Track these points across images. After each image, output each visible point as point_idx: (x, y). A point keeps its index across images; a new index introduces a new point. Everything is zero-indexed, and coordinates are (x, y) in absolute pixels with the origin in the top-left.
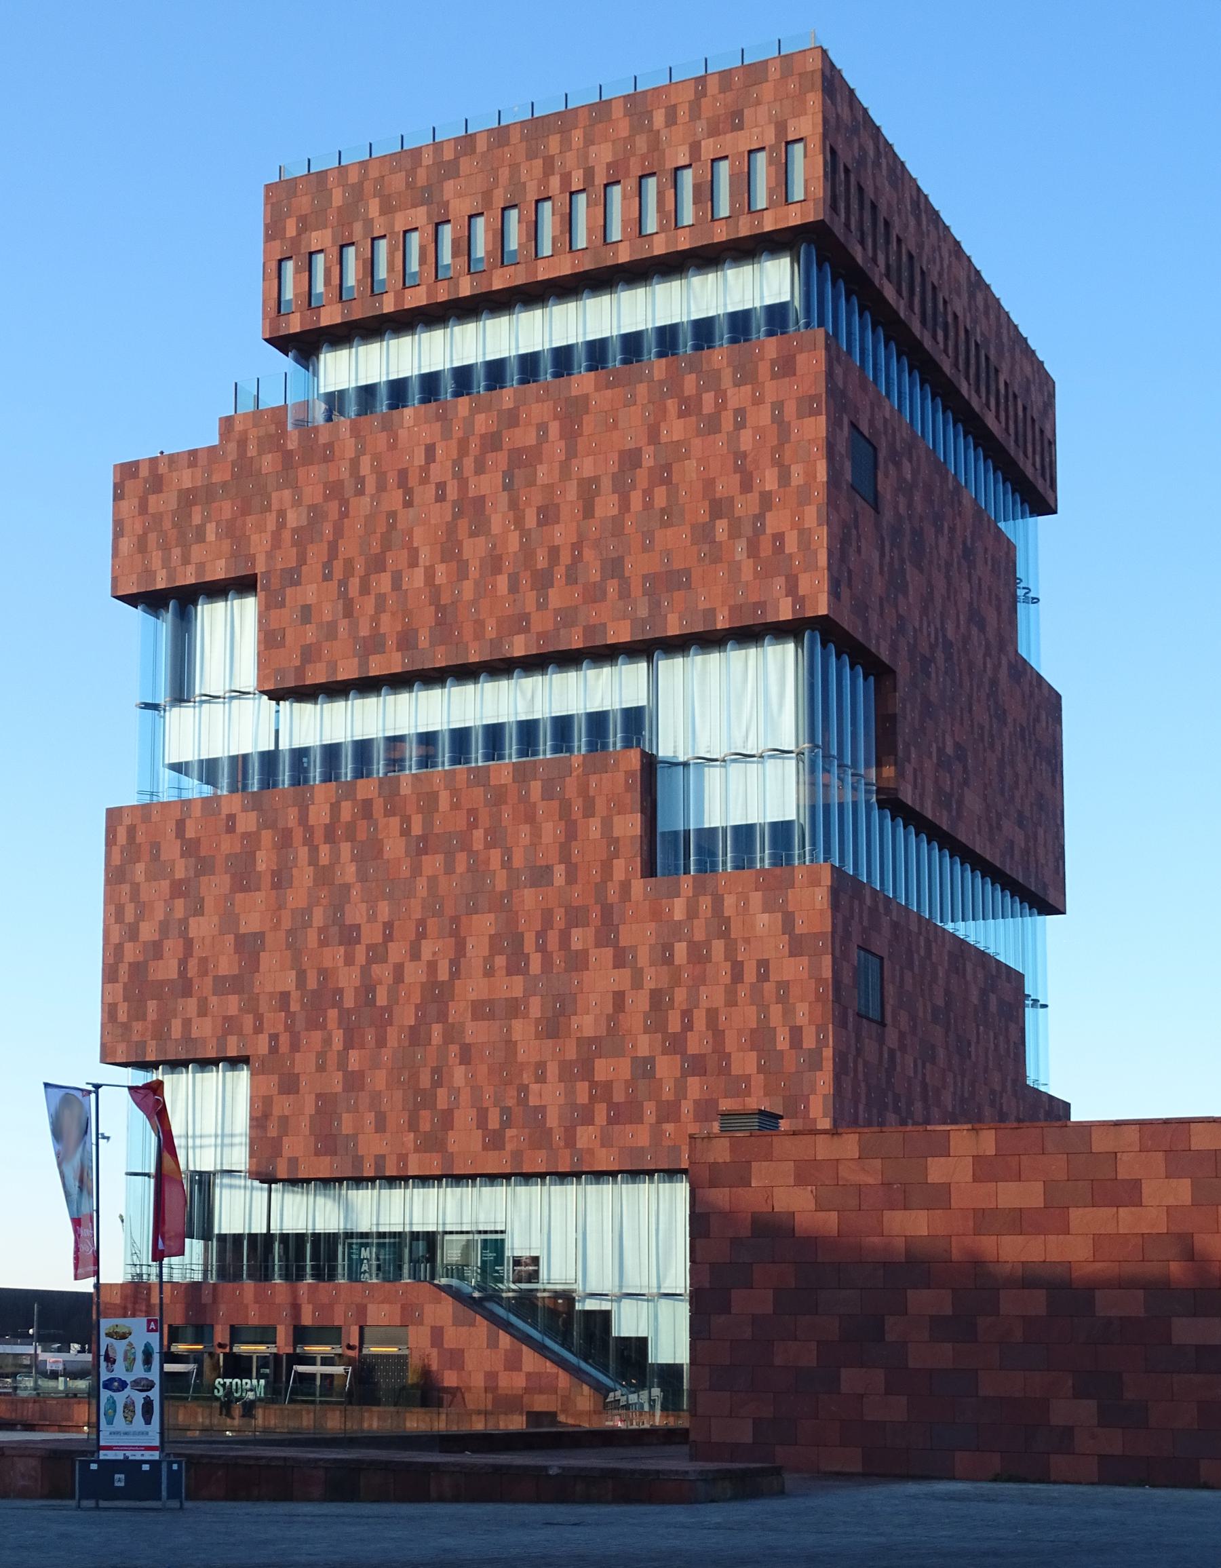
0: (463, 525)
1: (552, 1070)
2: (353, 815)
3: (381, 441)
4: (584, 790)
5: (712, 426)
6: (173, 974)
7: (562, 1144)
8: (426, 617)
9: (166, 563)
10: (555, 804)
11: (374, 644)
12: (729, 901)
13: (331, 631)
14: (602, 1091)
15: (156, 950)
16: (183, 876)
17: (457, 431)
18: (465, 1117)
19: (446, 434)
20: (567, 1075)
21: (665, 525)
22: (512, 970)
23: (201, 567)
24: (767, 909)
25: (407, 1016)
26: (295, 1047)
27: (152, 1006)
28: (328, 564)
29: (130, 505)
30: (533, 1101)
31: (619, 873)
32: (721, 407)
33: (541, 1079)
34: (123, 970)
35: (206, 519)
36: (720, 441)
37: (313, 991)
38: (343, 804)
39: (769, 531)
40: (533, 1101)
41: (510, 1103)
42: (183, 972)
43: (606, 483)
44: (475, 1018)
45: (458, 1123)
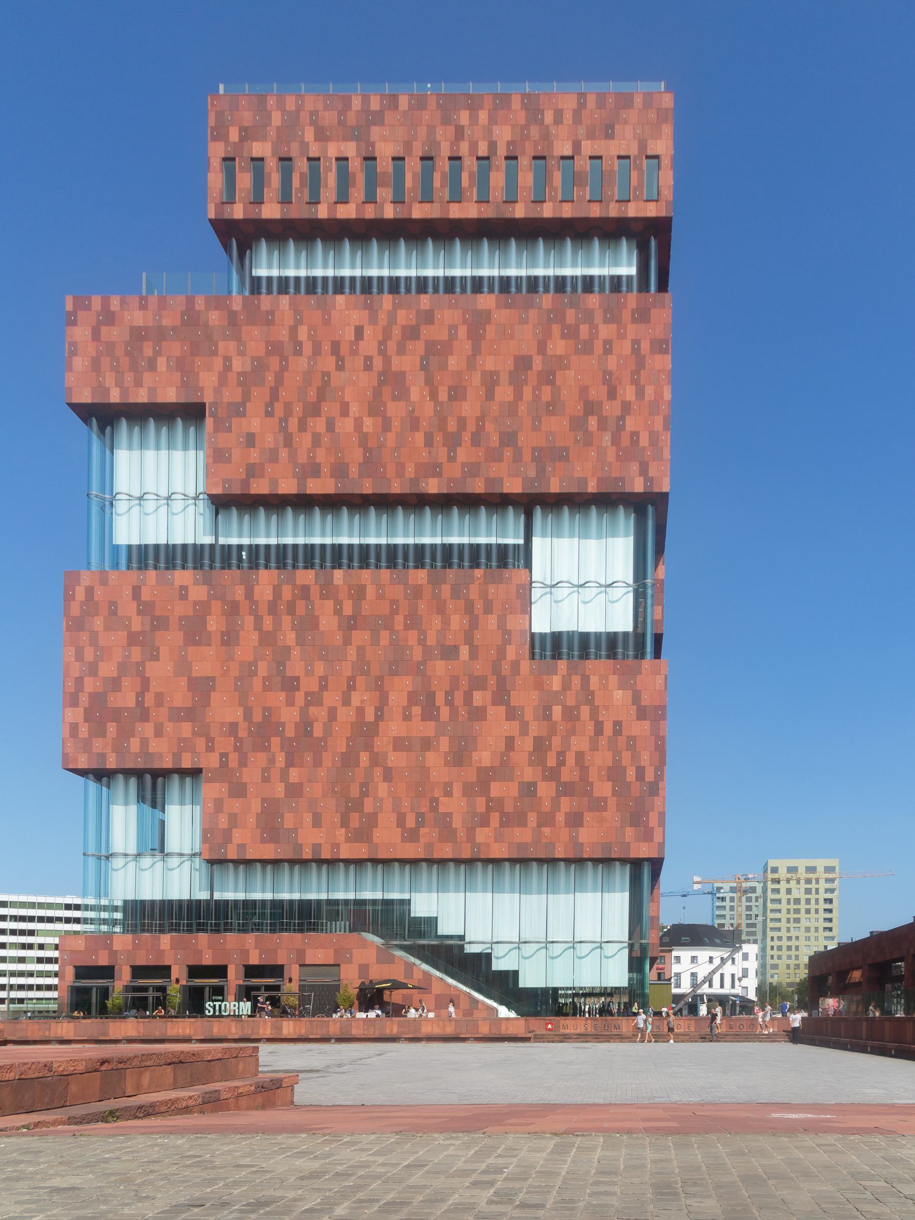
1: (457, 789)
4: (484, 595)
7: (465, 839)
8: (356, 455)
10: (462, 602)
11: (314, 470)
13: (273, 456)
17: (383, 318)
19: (373, 319)
20: (468, 791)
21: (550, 413)
23: (152, 391)
30: (442, 809)
35: (158, 354)
40: (442, 809)
43: (504, 378)
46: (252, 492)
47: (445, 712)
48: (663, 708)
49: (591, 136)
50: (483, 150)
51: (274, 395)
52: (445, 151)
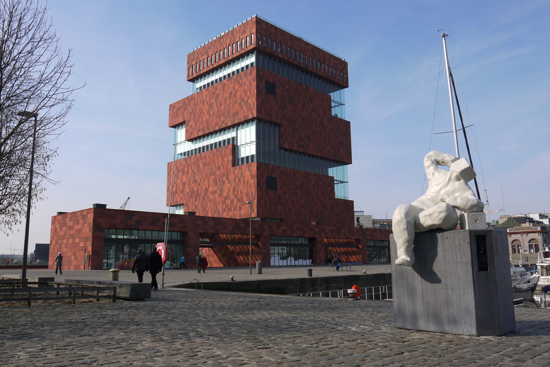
6: (175, 191)
11: (199, 131)
12: (243, 170)
23: (179, 120)
24: (248, 171)
28: (194, 118)
31: (229, 167)
32: (242, 82)
33: (219, 204)
36: (242, 88)
41: (215, 209)
42: (176, 190)
43: (228, 98)
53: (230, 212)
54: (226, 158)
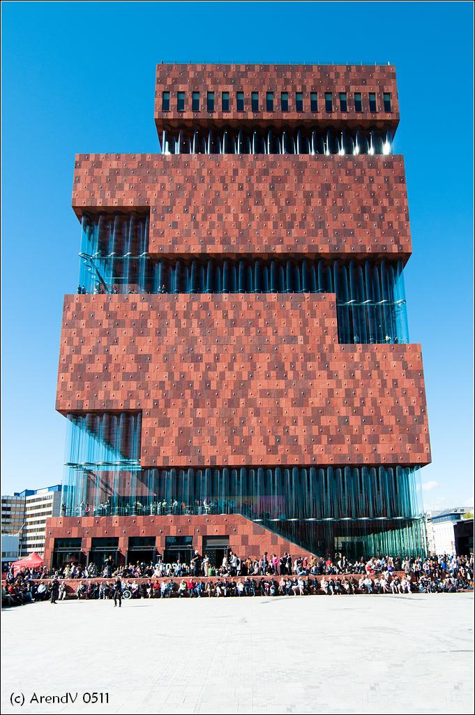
0: (251, 201)
1: (300, 422)
2: (198, 308)
3: (212, 164)
5: (360, 180)
9: (102, 196)
11: (209, 240)
12: (379, 356)
13: (188, 234)
14: (325, 430)
15: (91, 359)
16: (107, 327)
18: (257, 441)
19: (243, 166)
20: (307, 422)
22: (278, 378)
25: (227, 394)
26: (167, 406)
27: (87, 384)
29: (84, 171)
30: (291, 433)
33: (295, 423)
34: (71, 366)
37: (177, 382)
38: (194, 303)
39: (386, 220)
43: (316, 194)
44: (261, 396)
45: (254, 442)
46: (176, 252)
47: (290, 375)
48: (422, 371)
49: (354, 83)
50: (299, 89)
51: (189, 203)
52: (280, 89)
53: (338, 447)
54: (316, 321)
